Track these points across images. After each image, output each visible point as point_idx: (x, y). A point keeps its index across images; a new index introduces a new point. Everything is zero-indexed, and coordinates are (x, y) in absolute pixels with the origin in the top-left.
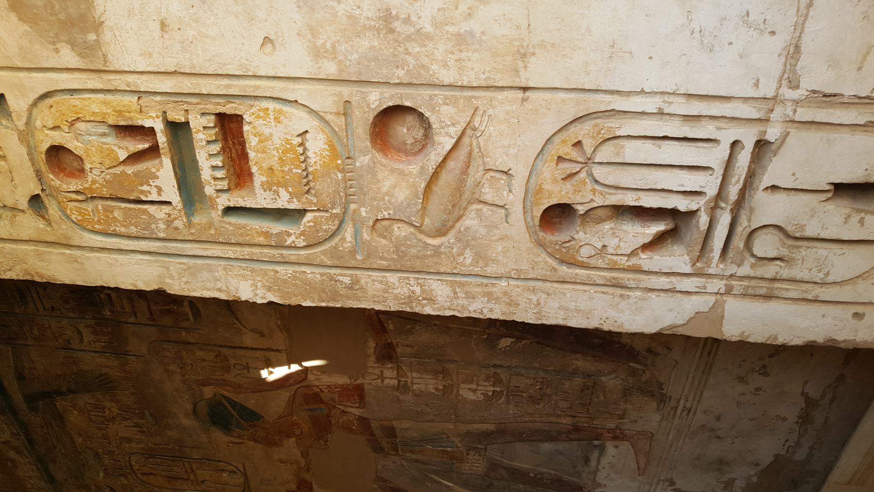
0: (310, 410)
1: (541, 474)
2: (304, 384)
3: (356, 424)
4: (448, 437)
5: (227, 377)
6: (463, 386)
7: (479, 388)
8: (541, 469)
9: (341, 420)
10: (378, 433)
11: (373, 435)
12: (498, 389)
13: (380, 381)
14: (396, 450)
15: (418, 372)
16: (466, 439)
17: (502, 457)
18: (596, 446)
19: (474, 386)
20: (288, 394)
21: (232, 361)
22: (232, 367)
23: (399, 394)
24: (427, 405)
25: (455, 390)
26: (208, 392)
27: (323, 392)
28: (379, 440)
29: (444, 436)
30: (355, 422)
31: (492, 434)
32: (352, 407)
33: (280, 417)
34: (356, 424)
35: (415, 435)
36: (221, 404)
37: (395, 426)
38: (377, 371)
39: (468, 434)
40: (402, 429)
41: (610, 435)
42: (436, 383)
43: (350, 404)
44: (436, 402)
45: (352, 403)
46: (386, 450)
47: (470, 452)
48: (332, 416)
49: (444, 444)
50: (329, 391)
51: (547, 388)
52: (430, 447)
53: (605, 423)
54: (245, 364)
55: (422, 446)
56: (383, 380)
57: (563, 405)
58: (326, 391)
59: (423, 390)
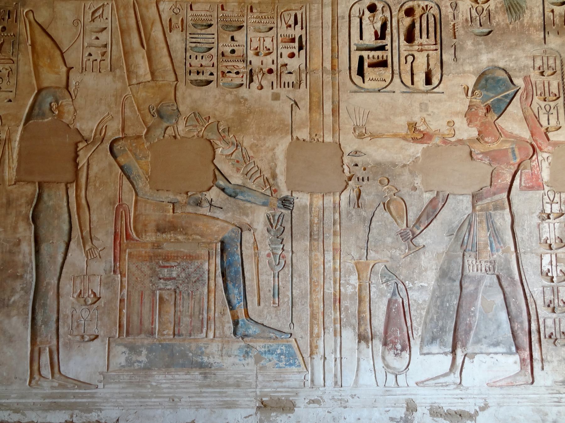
0: (513, 151)
1: (475, 316)
2: (538, 150)
3: (503, 182)
4: (501, 247)
5: (536, 98)
6: (554, 256)
7: (554, 268)
8: (478, 314)
9: (505, 172)
10: (497, 197)
11: (494, 194)
12: (555, 279)
13: (548, 201)
14: (481, 210)
15: (560, 227)
16: (502, 261)
17: (486, 286)
18: (510, 349)
19: (554, 263)
20: (528, 138)
21: (552, 104)
22: (546, 103)
23: (538, 213)
24: (530, 233)
25: (549, 251)
26: (519, 82)
27: (533, 162)
28: (489, 198)
29: (502, 245)
30: (505, 182)
31: (511, 278)
32: (521, 180)
33: (502, 129)
34: (503, 182)
35: (498, 224)
36: (508, 89)
37: (506, 210)
38: (557, 199)
39: (508, 261)
40: (503, 215)
41: (526, 356)
42: (552, 238)
43: (523, 180)
44: (535, 239)
45: (524, 181)
46: (479, 203)
47: (489, 264)
48: (508, 166)
49: (494, 244)
50: (534, 166)
51: (559, 310)
52: (488, 235)
53: (537, 351)
54: (551, 112)
55: (488, 229)
56: (547, 203)
57: (549, 322)
58: (534, 164)
59: (544, 230)
